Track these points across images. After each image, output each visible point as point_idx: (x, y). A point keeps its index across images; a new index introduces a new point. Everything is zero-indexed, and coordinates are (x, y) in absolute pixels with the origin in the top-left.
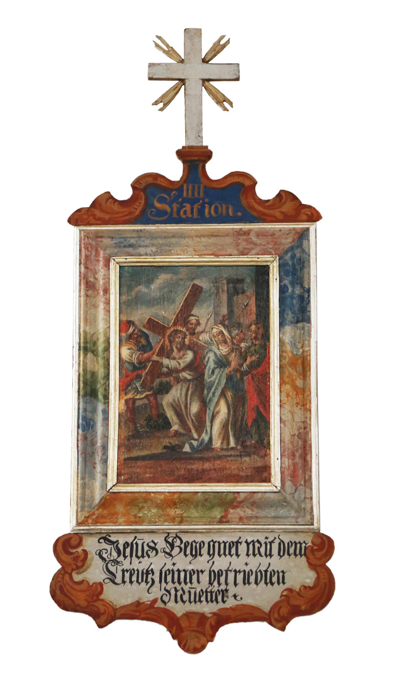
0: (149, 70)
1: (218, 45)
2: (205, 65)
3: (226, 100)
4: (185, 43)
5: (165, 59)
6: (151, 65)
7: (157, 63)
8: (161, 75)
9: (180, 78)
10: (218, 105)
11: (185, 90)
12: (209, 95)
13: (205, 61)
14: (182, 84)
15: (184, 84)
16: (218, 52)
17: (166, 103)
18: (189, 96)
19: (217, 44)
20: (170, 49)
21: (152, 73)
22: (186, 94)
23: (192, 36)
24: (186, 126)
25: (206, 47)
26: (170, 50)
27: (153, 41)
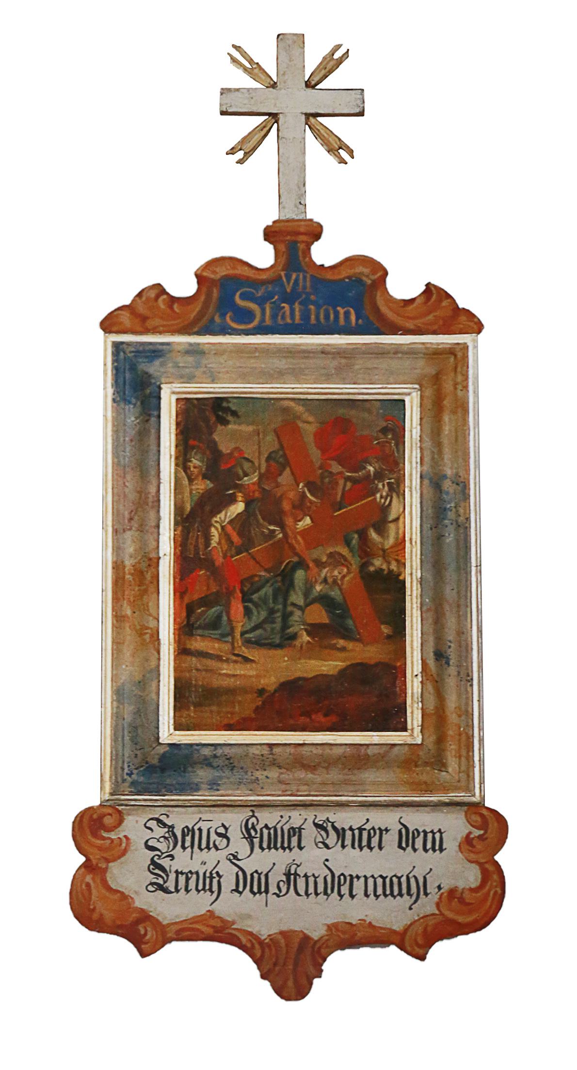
0: (221, 99)
1: (330, 61)
2: (310, 90)
3: (343, 146)
4: (279, 57)
5: (246, 82)
6: (224, 92)
7: (235, 89)
8: (240, 108)
9: (270, 111)
10: (331, 155)
11: (278, 130)
12: (316, 138)
13: (309, 85)
14: (273, 121)
15: (277, 122)
16: (331, 72)
17: (248, 151)
18: (284, 140)
19: (329, 59)
20: (254, 66)
21: (227, 104)
22: (280, 138)
23: (289, 46)
24: (280, 187)
25: (312, 61)
26: (255, 68)
27: (228, 54)
